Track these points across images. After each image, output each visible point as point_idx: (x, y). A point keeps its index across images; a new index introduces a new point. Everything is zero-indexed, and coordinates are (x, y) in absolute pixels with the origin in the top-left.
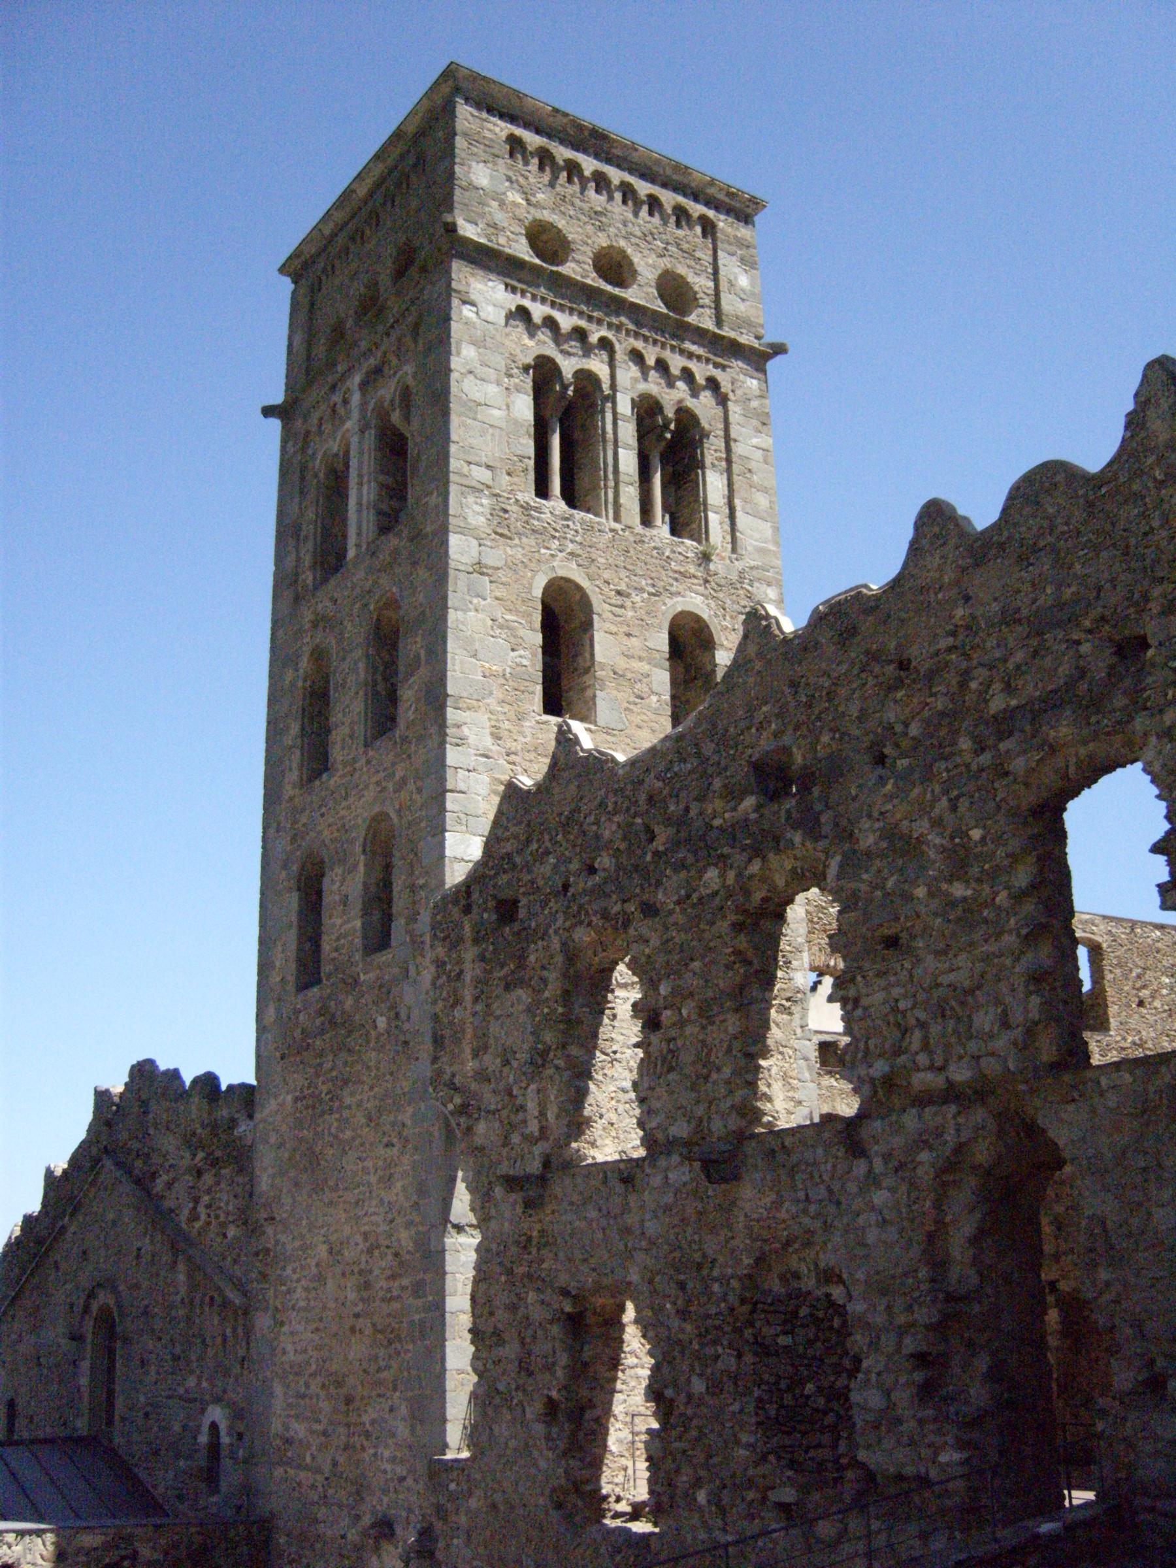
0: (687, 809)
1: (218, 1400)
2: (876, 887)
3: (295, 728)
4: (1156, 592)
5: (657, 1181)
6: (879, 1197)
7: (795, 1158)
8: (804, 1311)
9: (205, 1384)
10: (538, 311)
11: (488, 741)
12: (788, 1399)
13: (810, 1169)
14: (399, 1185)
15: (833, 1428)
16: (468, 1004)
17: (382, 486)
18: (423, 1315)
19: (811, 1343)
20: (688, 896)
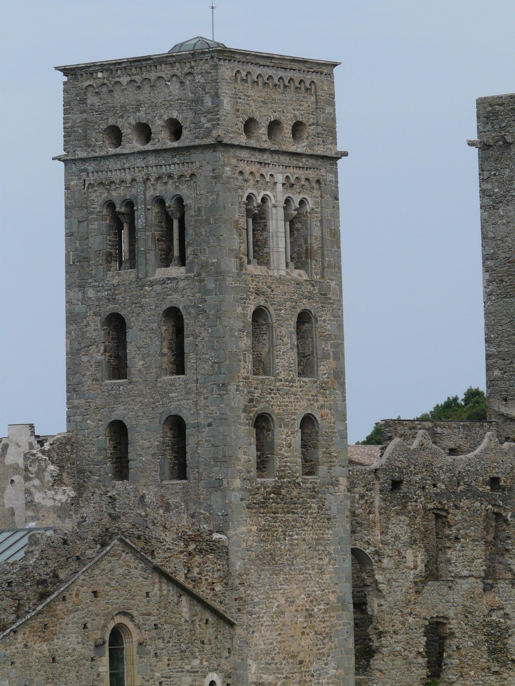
1: (215, 670)
9: (205, 663)
12: (494, 646)
18: (342, 627)
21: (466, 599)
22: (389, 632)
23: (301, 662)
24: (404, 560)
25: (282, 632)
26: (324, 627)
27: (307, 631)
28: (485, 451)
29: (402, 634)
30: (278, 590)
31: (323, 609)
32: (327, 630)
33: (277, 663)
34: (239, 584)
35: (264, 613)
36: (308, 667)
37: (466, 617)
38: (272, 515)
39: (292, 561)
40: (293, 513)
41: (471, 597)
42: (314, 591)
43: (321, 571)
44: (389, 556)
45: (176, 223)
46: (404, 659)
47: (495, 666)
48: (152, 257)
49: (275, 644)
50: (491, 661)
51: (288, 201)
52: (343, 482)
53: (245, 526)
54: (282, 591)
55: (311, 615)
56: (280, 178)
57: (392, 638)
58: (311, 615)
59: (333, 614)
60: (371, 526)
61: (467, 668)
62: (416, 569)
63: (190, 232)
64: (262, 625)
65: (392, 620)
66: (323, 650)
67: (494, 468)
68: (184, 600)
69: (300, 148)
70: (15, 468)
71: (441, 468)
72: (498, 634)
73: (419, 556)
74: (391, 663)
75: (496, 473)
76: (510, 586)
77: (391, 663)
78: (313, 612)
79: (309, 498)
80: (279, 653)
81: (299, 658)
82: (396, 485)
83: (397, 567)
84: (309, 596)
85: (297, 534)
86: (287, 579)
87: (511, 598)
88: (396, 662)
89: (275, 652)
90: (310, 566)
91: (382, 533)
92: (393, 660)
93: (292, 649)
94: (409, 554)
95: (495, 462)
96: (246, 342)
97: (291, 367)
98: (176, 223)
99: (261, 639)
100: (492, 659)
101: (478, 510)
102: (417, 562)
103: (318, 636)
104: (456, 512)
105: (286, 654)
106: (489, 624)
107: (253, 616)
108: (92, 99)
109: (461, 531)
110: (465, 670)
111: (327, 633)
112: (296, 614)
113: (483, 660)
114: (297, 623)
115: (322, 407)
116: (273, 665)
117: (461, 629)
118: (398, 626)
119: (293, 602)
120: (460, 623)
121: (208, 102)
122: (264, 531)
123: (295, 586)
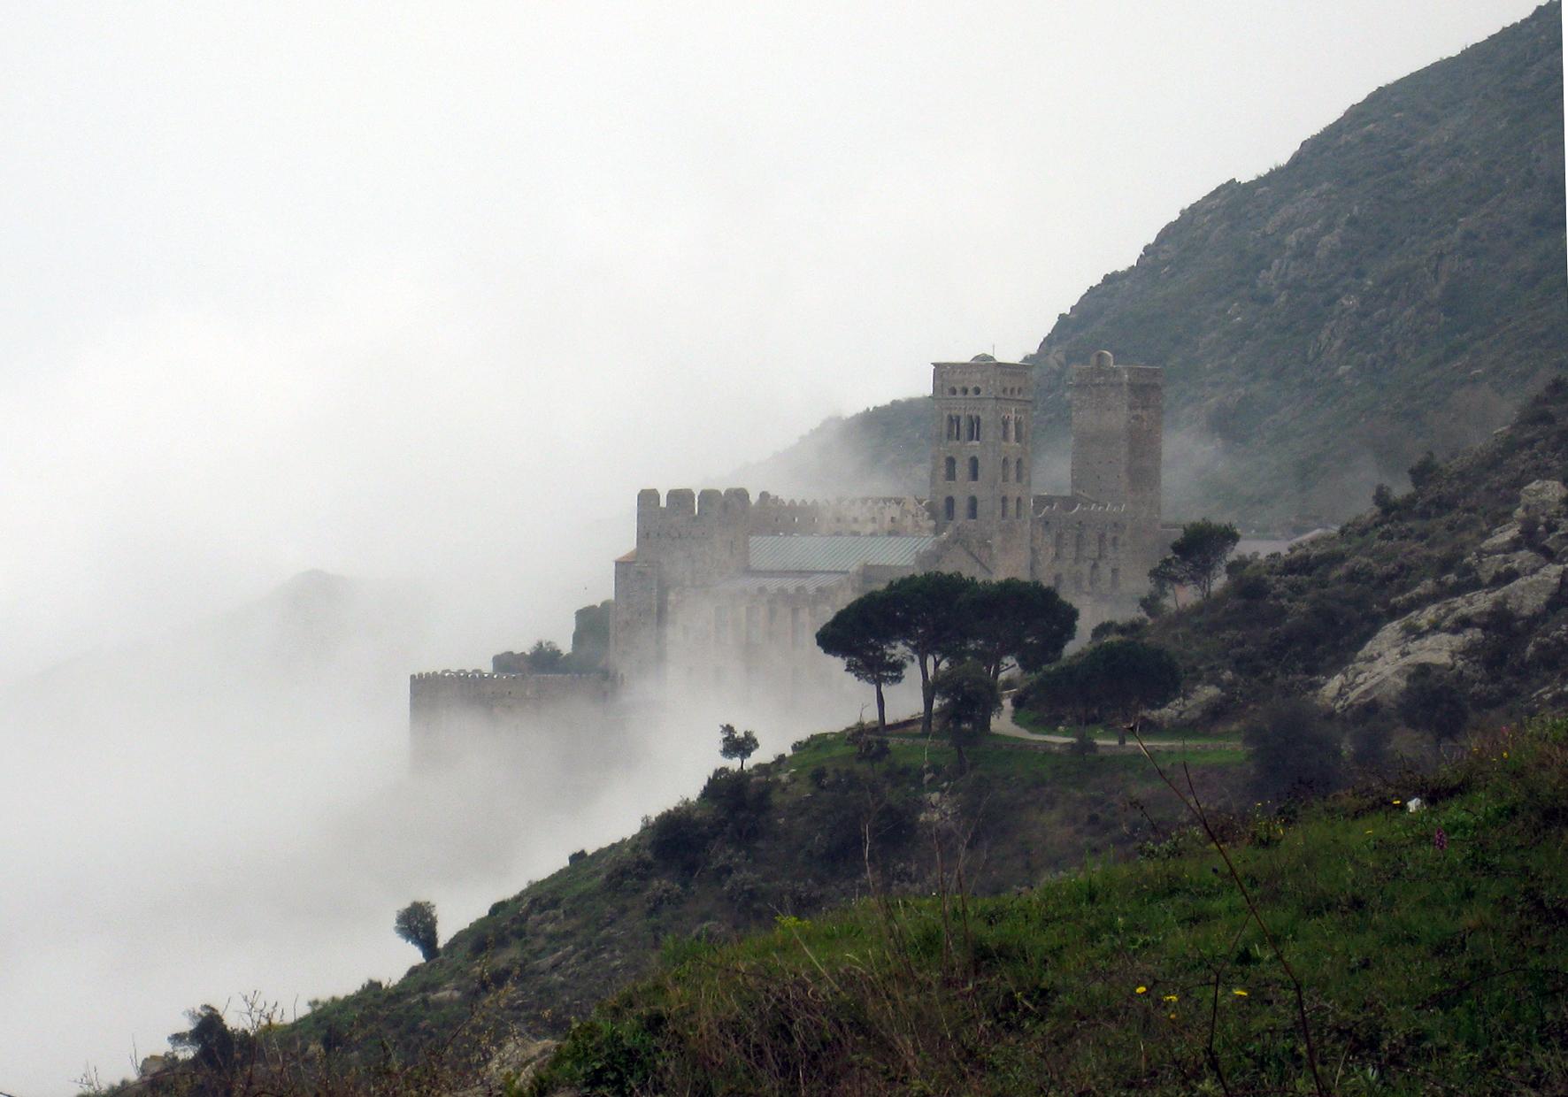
28: (1078, 511)
45: (975, 425)
48: (966, 436)
51: (1016, 418)
52: (1029, 522)
56: (1013, 409)
60: (1038, 539)
63: (982, 429)
68: (978, 564)
69: (1020, 397)
70: (909, 511)
82: (1047, 523)
94: (1050, 549)
96: (1000, 471)
98: (975, 425)
108: (945, 376)
121: (992, 382)
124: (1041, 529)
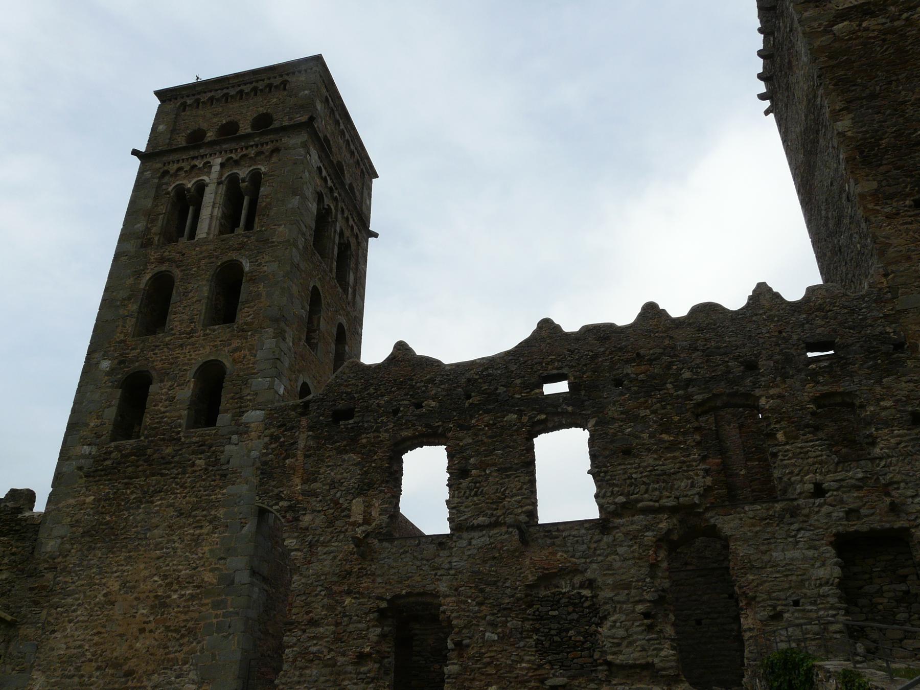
0: (497, 389)
2: (619, 431)
3: (134, 307)
4: (764, 352)
5: (464, 543)
6: (621, 550)
7: (564, 534)
8: (564, 600)
10: (324, 173)
11: (291, 344)
12: (557, 639)
13: (576, 539)
14: (206, 549)
15: (588, 649)
16: (301, 458)
17: (223, 213)
19: (569, 614)
20: (495, 424)
21: (478, 561)
22: (299, 623)
23: (129, 674)
24: (344, 513)
25: (103, 630)
26: (184, 621)
27: (152, 626)
29: (327, 625)
30: (112, 573)
31: (189, 594)
32: (190, 624)
33: (83, 676)
34: (45, 569)
35: (79, 605)
36: (140, 680)
37: (482, 591)
38: (126, 481)
39: (146, 534)
40: (162, 475)
41: (494, 558)
42: (180, 571)
43: (197, 541)
44: (314, 511)
46: (326, 666)
47: (554, 675)
49: (87, 647)
50: (547, 667)
53: (74, 497)
54: (118, 574)
55: (164, 605)
57: (304, 631)
58: (164, 605)
59: (205, 601)
61: (481, 681)
62: (370, 524)
64: (70, 622)
65: (307, 604)
66: (177, 654)
67: (552, 361)
71: (431, 381)
72: (575, 616)
73: (377, 505)
74: (297, 673)
75: (557, 369)
76: (598, 531)
77: (297, 673)
78: (168, 601)
79: (194, 453)
80: (91, 661)
81: (126, 668)
83: (331, 524)
84: (165, 577)
85: (161, 499)
86: (130, 557)
87: (598, 552)
88: (308, 672)
89: (83, 659)
90: (176, 538)
91: (305, 482)
92: (300, 668)
93: (115, 654)
95: (551, 354)
97: (194, 319)
99: (63, 641)
100: (550, 662)
101: (515, 425)
102: (370, 514)
103: (170, 634)
104: (460, 435)
105: (102, 662)
106: (555, 602)
107: (59, 609)
109: (472, 460)
110: (478, 683)
111: (189, 628)
112: (135, 603)
113: (524, 665)
114: (135, 617)
115: (237, 349)
116: (76, 679)
117: (468, 611)
118: (319, 611)
119: (134, 587)
120: (465, 602)
122: (105, 500)
123: (142, 566)
124: (303, 439)
